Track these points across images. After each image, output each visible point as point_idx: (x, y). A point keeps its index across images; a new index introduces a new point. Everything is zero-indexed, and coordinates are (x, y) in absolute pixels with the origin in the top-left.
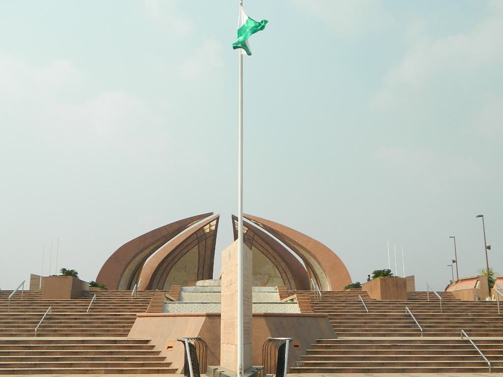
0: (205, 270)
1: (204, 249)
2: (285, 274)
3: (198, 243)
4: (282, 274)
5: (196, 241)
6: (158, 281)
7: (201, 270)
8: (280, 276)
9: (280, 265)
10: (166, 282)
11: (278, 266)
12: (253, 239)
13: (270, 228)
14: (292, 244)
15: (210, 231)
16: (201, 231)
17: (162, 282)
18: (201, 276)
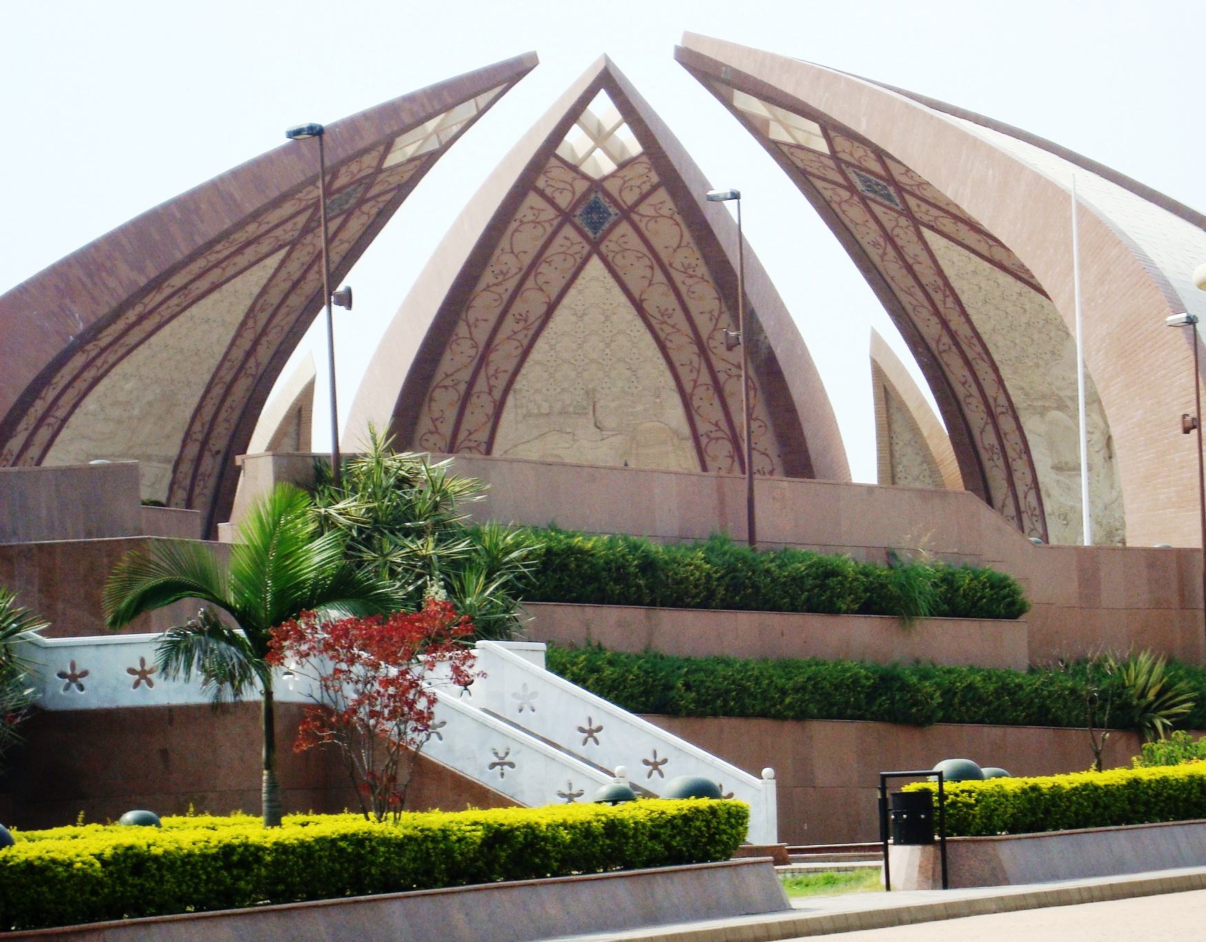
1: (659, 276)
5: (568, 231)
7: (710, 411)
15: (622, 166)
16: (556, 171)
18: (727, 446)
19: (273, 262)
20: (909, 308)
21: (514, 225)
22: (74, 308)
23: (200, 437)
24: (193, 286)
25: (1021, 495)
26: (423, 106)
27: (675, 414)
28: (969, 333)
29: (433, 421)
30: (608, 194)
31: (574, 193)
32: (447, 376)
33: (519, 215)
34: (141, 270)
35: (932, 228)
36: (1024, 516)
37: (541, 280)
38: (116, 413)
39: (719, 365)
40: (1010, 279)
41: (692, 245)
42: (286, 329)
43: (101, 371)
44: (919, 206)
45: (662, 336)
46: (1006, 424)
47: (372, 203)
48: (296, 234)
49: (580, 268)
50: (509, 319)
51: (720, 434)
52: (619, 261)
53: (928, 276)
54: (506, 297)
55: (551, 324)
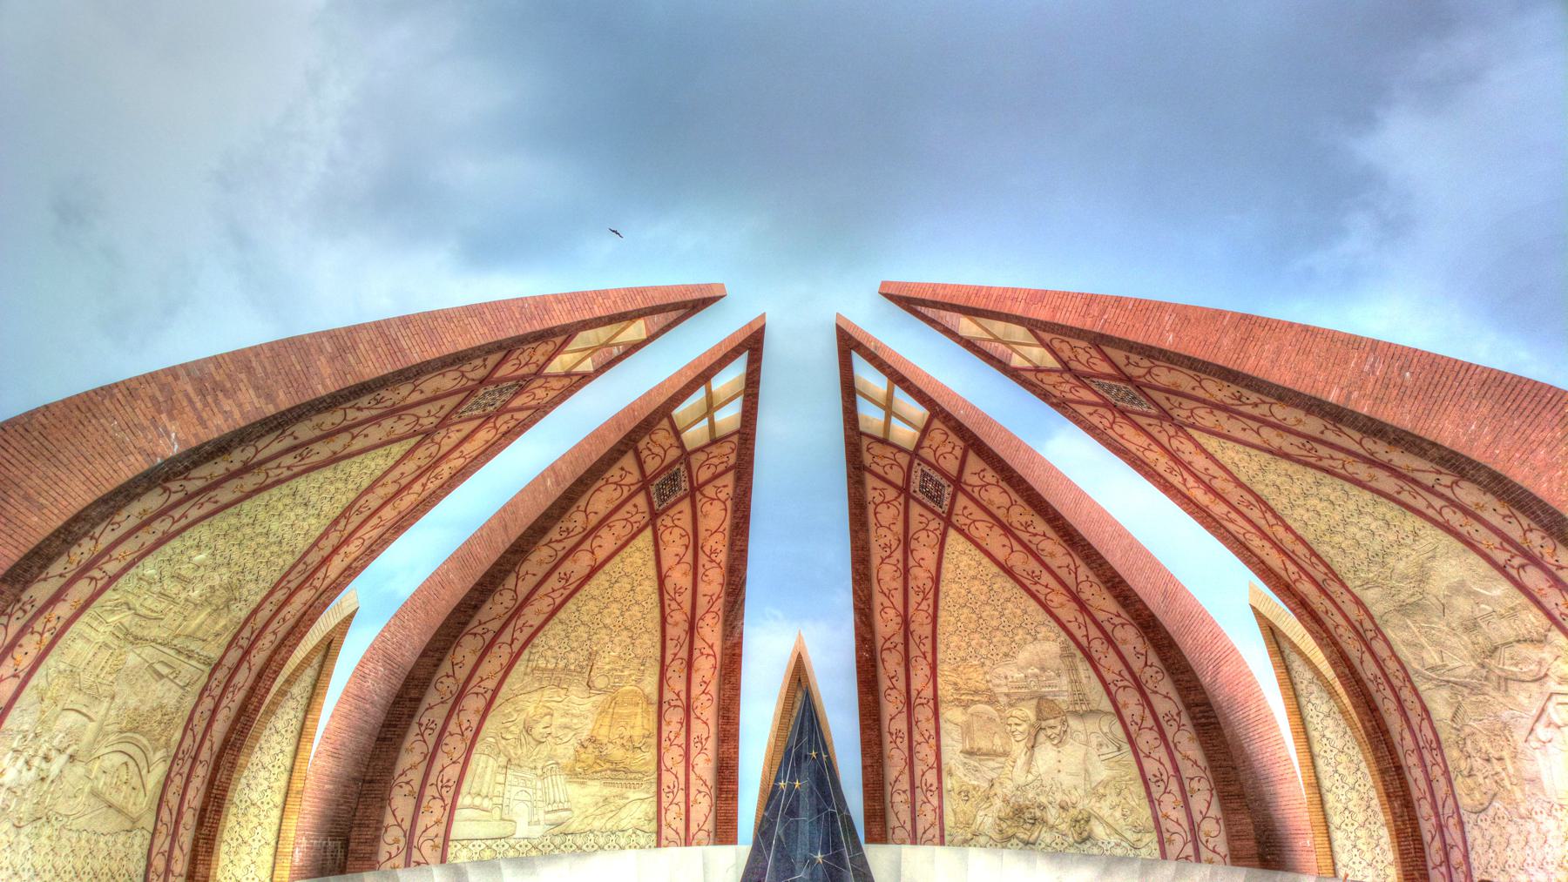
0: (696, 679)
1: (689, 557)
2: (1138, 696)
3: (655, 515)
4: (1121, 697)
5: (640, 500)
6: (431, 741)
8: (1106, 705)
9: (1110, 641)
10: (479, 746)
11: (1098, 646)
12: (957, 483)
13: (1099, 341)
15: (715, 441)
16: (662, 436)
17: (455, 745)
22: (173, 428)
23: (245, 643)
24: (316, 447)
25: (918, 772)
26: (615, 302)
27: (650, 685)
28: (928, 630)
30: (689, 468)
33: (608, 475)
34: (270, 397)
35: (961, 531)
36: (918, 791)
38: (172, 588)
39: (698, 644)
40: (1009, 584)
42: (367, 543)
43: (176, 527)
45: (668, 610)
46: (923, 713)
47: (507, 417)
49: (634, 537)
50: (555, 576)
52: (666, 536)
53: (921, 577)
54: (561, 554)
55: (586, 587)
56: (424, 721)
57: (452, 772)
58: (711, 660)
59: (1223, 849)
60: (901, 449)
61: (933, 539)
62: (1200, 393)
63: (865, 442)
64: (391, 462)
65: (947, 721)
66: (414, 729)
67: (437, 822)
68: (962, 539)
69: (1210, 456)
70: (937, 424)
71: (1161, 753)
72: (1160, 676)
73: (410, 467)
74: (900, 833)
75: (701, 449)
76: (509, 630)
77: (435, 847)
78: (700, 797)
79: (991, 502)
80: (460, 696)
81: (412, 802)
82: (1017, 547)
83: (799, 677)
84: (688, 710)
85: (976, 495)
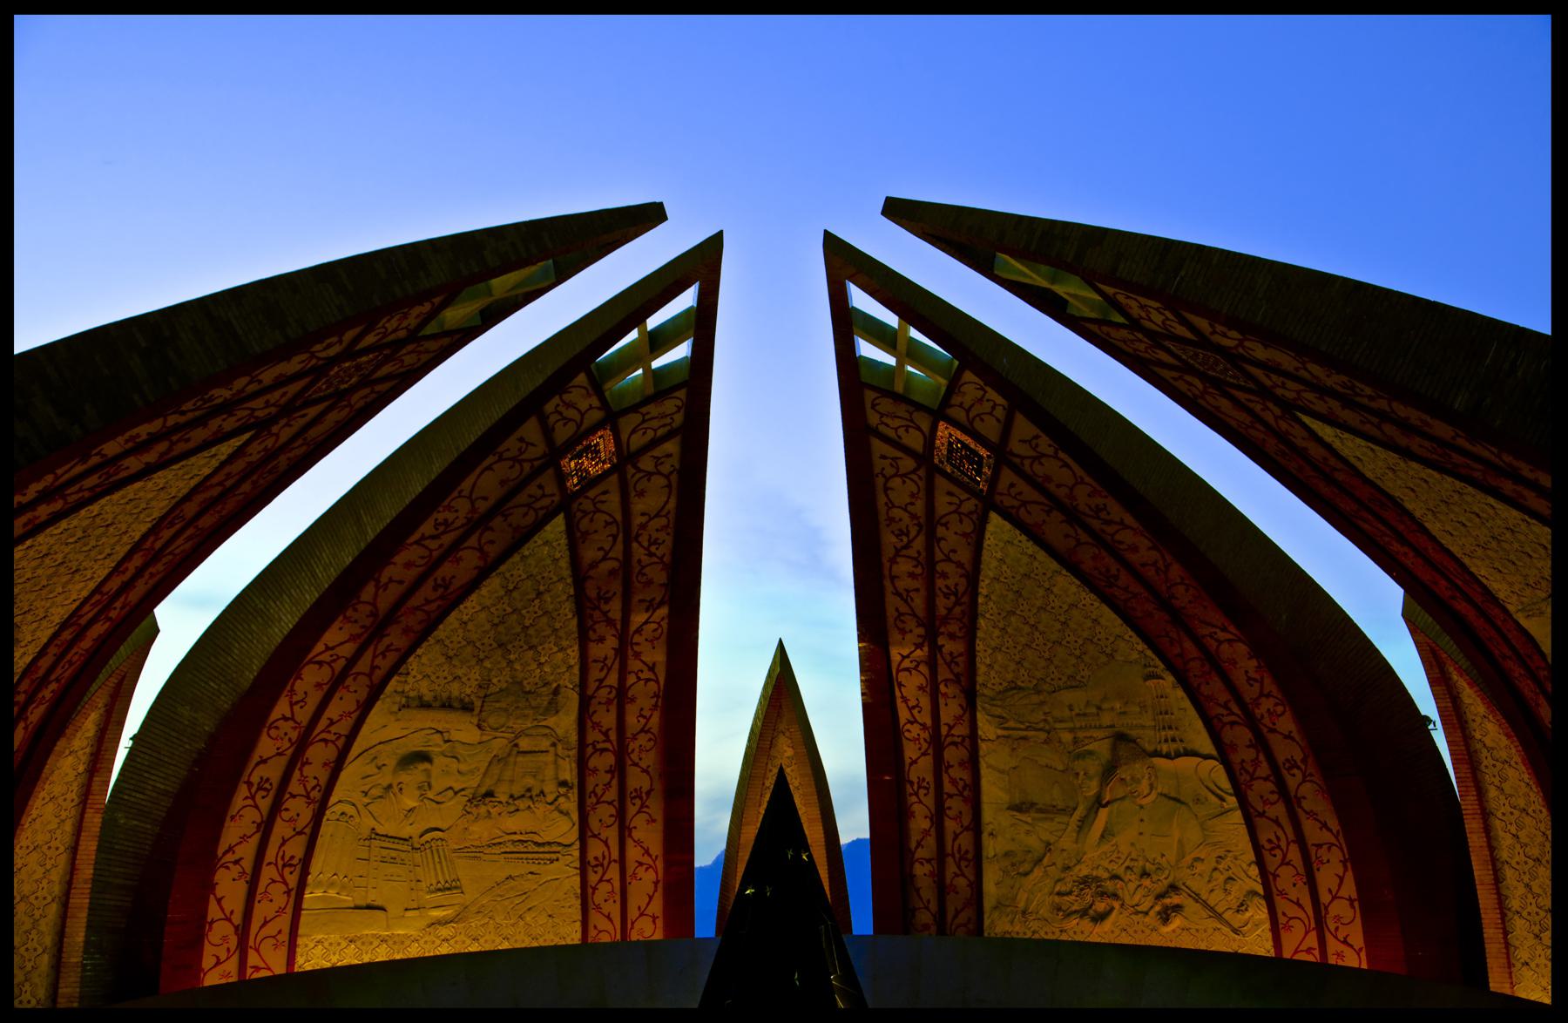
2: (1250, 735)
4: (1228, 735)
5: (547, 479)
6: (265, 804)
12: (1001, 452)
14: (1373, 461)
16: (579, 395)
17: (298, 809)
19: (225, 449)
20: (891, 612)
21: (490, 460)
29: (292, 705)
31: (579, 426)
32: (328, 648)
33: (501, 449)
35: (1006, 515)
36: (950, 860)
37: (488, 535)
39: (634, 665)
41: (671, 516)
44: (1012, 485)
47: (366, 391)
48: (273, 410)
50: (430, 582)
51: (608, 745)
56: (255, 779)
57: (296, 849)
58: (652, 686)
59: (1358, 940)
60: (919, 407)
61: (968, 527)
62: (1303, 373)
63: (869, 395)
64: (215, 463)
65: (989, 766)
66: (243, 791)
67: (280, 911)
68: (1008, 526)
69: (1328, 447)
70: (968, 376)
71: (1279, 810)
72: (1280, 709)
73: (240, 465)
74: (924, 917)
75: (634, 408)
76: (368, 655)
77: (276, 946)
78: (641, 871)
79: (1048, 479)
80: (302, 744)
81: (242, 888)
82: (1084, 537)
83: (782, 697)
84: (621, 753)
85: (1027, 468)
